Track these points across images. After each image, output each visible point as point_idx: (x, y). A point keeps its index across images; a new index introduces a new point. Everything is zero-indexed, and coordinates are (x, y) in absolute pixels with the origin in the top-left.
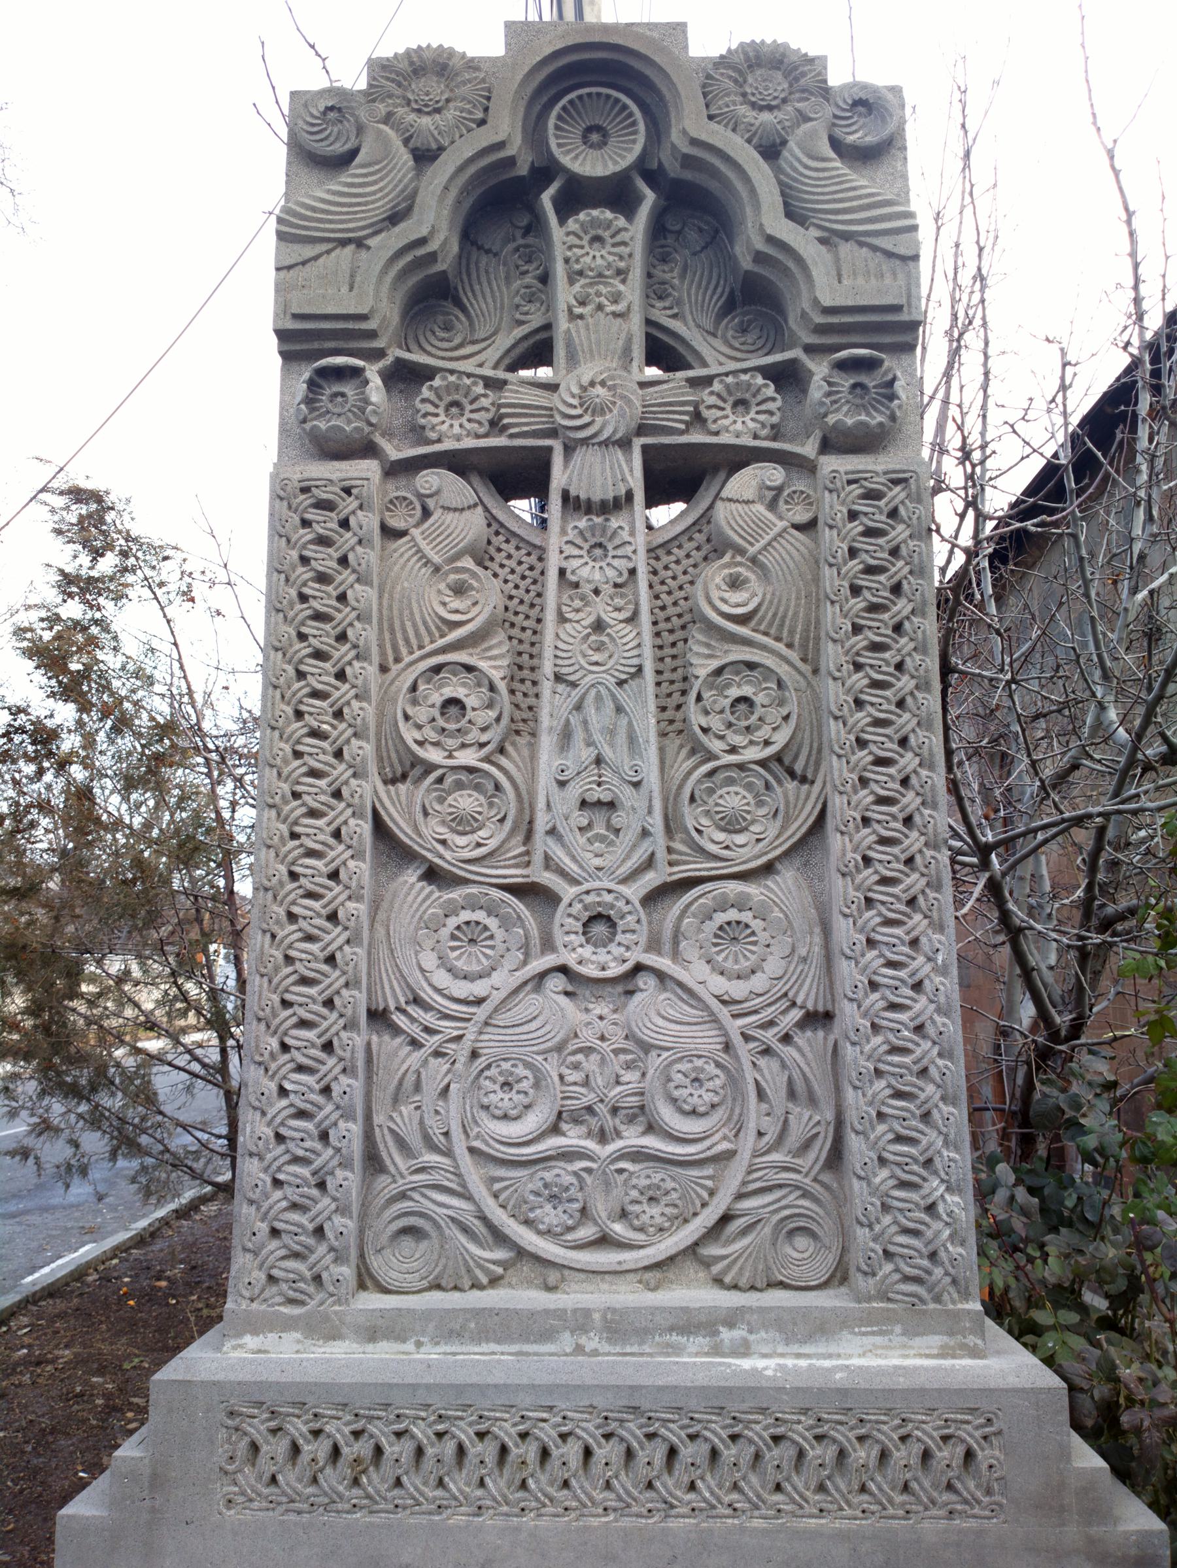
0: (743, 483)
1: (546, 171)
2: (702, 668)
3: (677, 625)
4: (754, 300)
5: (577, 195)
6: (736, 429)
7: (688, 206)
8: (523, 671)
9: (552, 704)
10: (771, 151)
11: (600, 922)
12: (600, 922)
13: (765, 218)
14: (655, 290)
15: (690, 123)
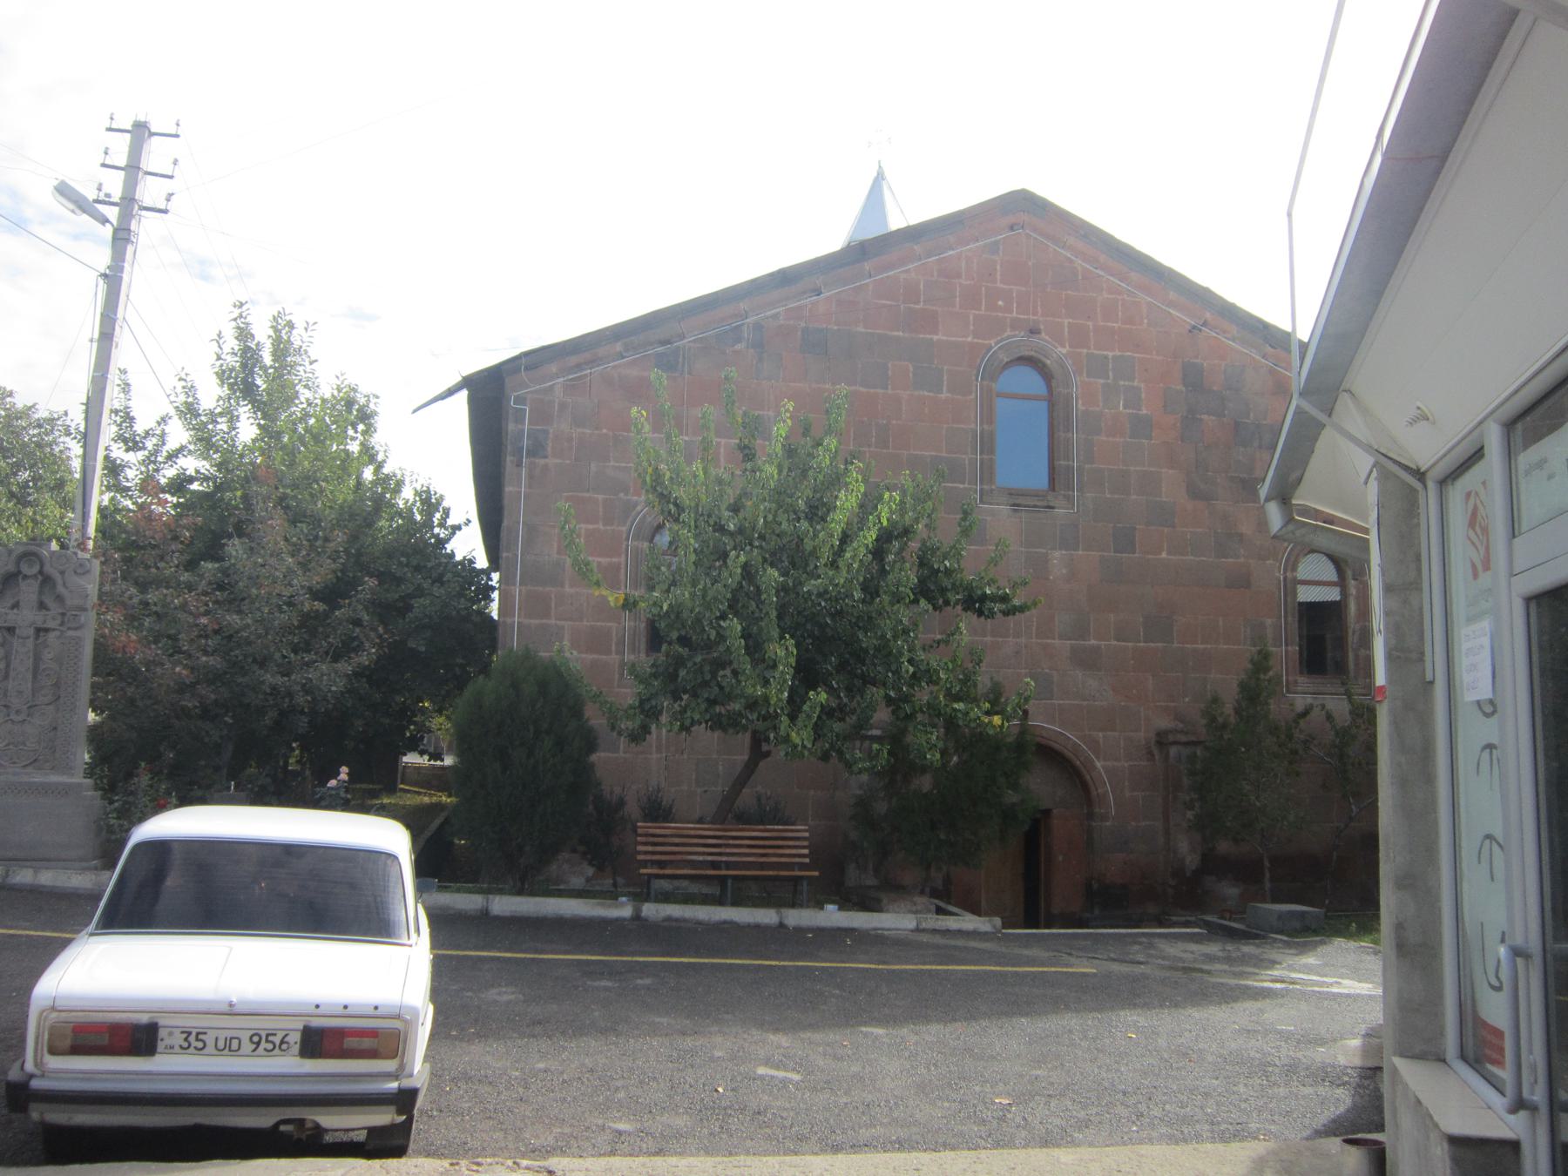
0: (52, 635)
1: (19, 572)
2: (42, 667)
3: (37, 658)
4: (59, 599)
5: (25, 577)
6: (50, 624)
7: (46, 581)
8: (8, 666)
9: (12, 674)
10: (62, 573)
11: (18, 712)
12: (18, 712)
13: (60, 589)
14: (41, 592)
15: (48, 569)
